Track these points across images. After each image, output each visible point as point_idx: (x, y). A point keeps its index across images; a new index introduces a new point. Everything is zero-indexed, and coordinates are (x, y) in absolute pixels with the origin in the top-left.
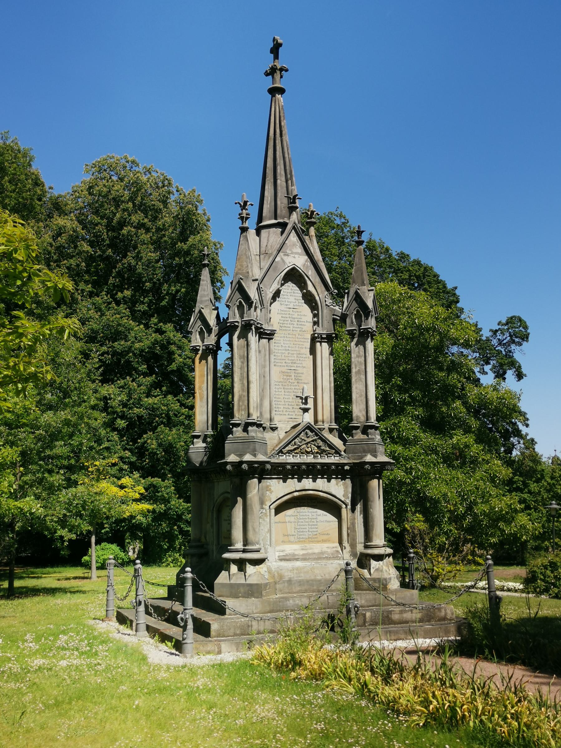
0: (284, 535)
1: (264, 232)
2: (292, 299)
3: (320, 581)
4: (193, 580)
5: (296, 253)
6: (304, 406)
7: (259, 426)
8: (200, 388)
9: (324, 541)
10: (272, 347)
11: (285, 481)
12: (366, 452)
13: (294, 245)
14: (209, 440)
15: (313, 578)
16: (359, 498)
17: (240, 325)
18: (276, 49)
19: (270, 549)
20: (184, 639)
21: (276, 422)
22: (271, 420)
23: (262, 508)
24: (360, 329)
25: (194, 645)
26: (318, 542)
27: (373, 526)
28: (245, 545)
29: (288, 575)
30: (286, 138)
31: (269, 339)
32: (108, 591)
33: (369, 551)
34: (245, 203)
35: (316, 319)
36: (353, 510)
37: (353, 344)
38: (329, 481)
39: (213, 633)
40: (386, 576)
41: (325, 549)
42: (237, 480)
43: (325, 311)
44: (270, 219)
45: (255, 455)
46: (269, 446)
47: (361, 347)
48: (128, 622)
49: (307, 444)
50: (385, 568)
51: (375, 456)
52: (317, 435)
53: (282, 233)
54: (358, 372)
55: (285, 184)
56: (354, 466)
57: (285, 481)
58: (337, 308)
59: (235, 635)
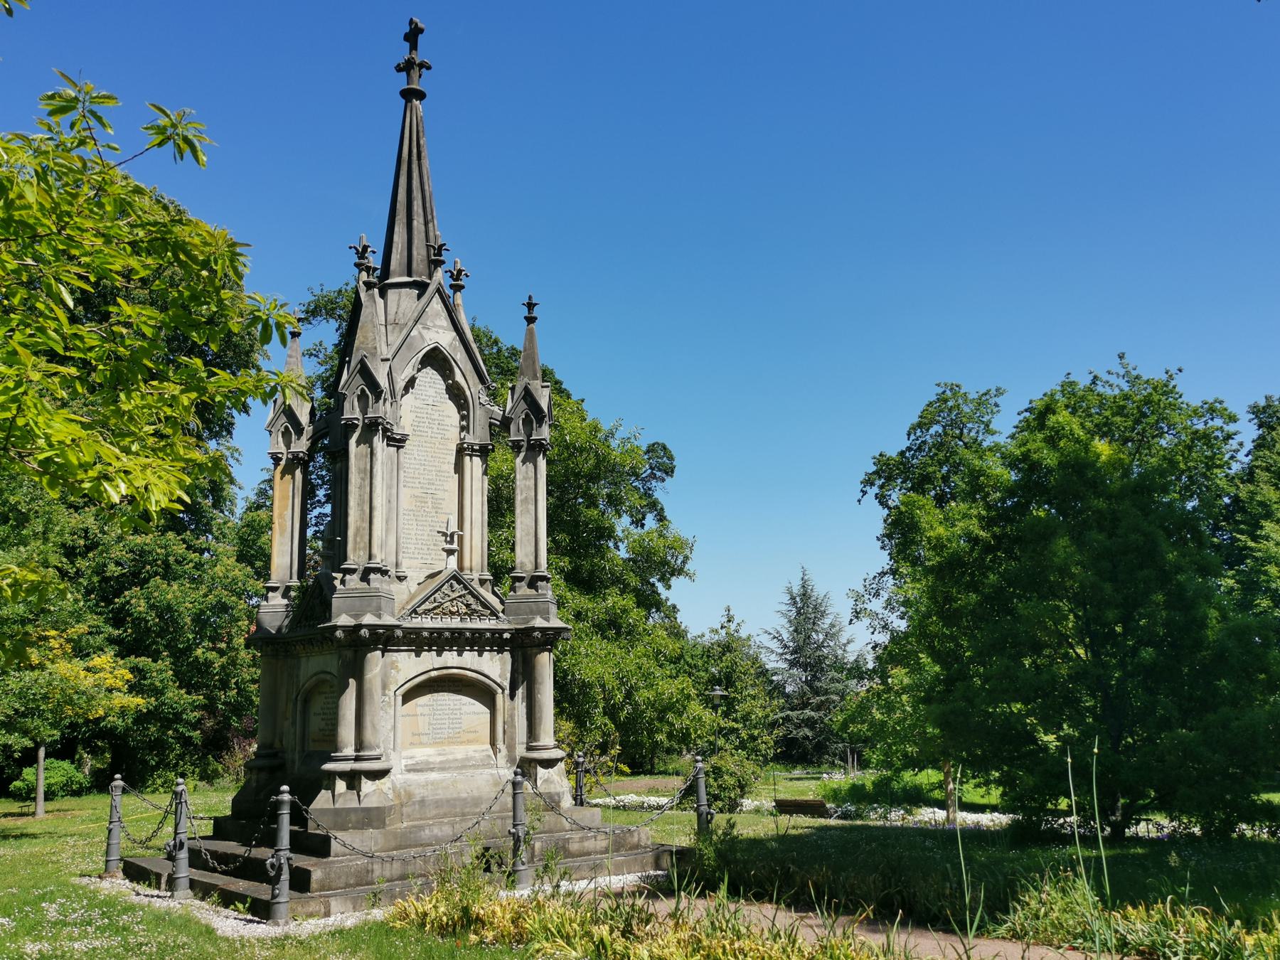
0: (414, 735)
1: (392, 294)
2: (431, 392)
3: (465, 799)
4: (293, 804)
5: (440, 327)
6: (448, 546)
7: (384, 573)
8: (281, 516)
9: (469, 742)
10: (401, 459)
11: (418, 655)
12: (534, 613)
13: (437, 315)
14: (293, 594)
15: (455, 796)
16: (520, 678)
17: (361, 424)
18: (413, 35)
19: (393, 755)
20: (274, 897)
21: (405, 569)
22: (397, 565)
23: (384, 694)
24: (529, 441)
25: (289, 905)
26: (462, 743)
27: (540, 719)
28: (357, 750)
29: (419, 793)
30: (426, 163)
31: (399, 448)
32: (110, 831)
33: (535, 755)
34: (365, 248)
35: (464, 423)
36: (512, 696)
37: (519, 460)
38: (480, 655)
39: (314, 885)
40: (559, 789)
41: (471, 754)
42: (349, 654)
43: (478, 412)
44: (401, 275)
45: (379, 616)
46: (396, 603)
47: (531, 466)
48: (153, 877)
49: (452, 601)
50: (556, 778)
51: (547, 620)
52: (466, 588)
53: (419, 297)
54: (525, 500)
55: (423, 227)
56: (517, 633)
57: (418, 655)
58: (496, 408)
59: (348, 885)
